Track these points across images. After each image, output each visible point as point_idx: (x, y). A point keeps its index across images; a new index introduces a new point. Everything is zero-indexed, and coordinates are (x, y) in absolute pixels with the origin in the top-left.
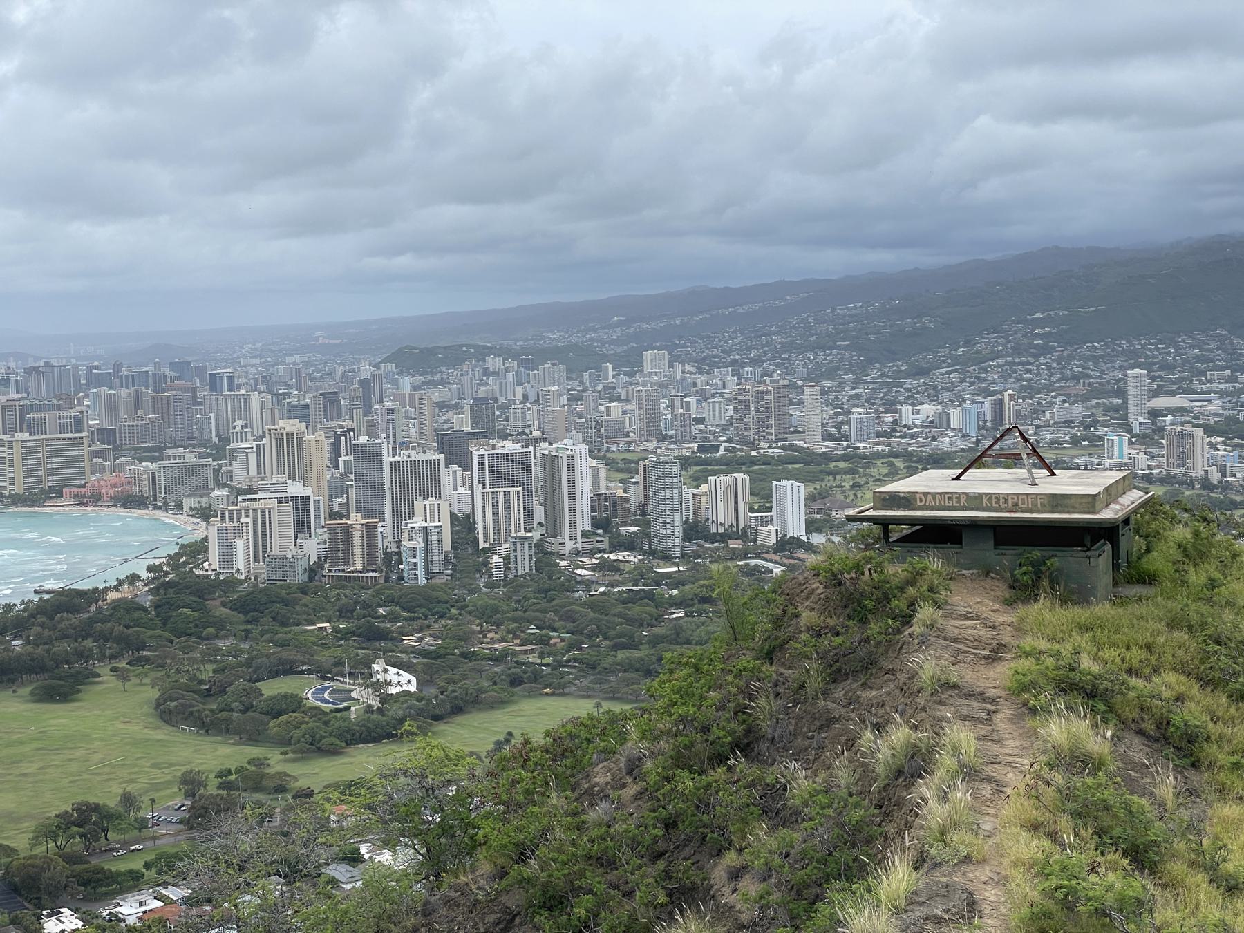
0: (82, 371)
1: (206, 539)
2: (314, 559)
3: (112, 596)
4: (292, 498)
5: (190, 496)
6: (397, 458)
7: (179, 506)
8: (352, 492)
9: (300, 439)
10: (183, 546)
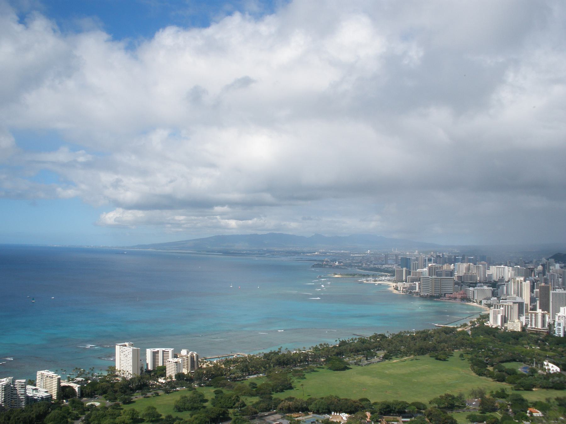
0: (453, 257)
1: (489, 314)
2: (524, 324)
3: (459, 330)
4: (518, 303)
5: (484, 299)
6: (555, 292)
7: (481, 302)
8: (538, 302)
9: (521, 283)
10: (481, 316)
